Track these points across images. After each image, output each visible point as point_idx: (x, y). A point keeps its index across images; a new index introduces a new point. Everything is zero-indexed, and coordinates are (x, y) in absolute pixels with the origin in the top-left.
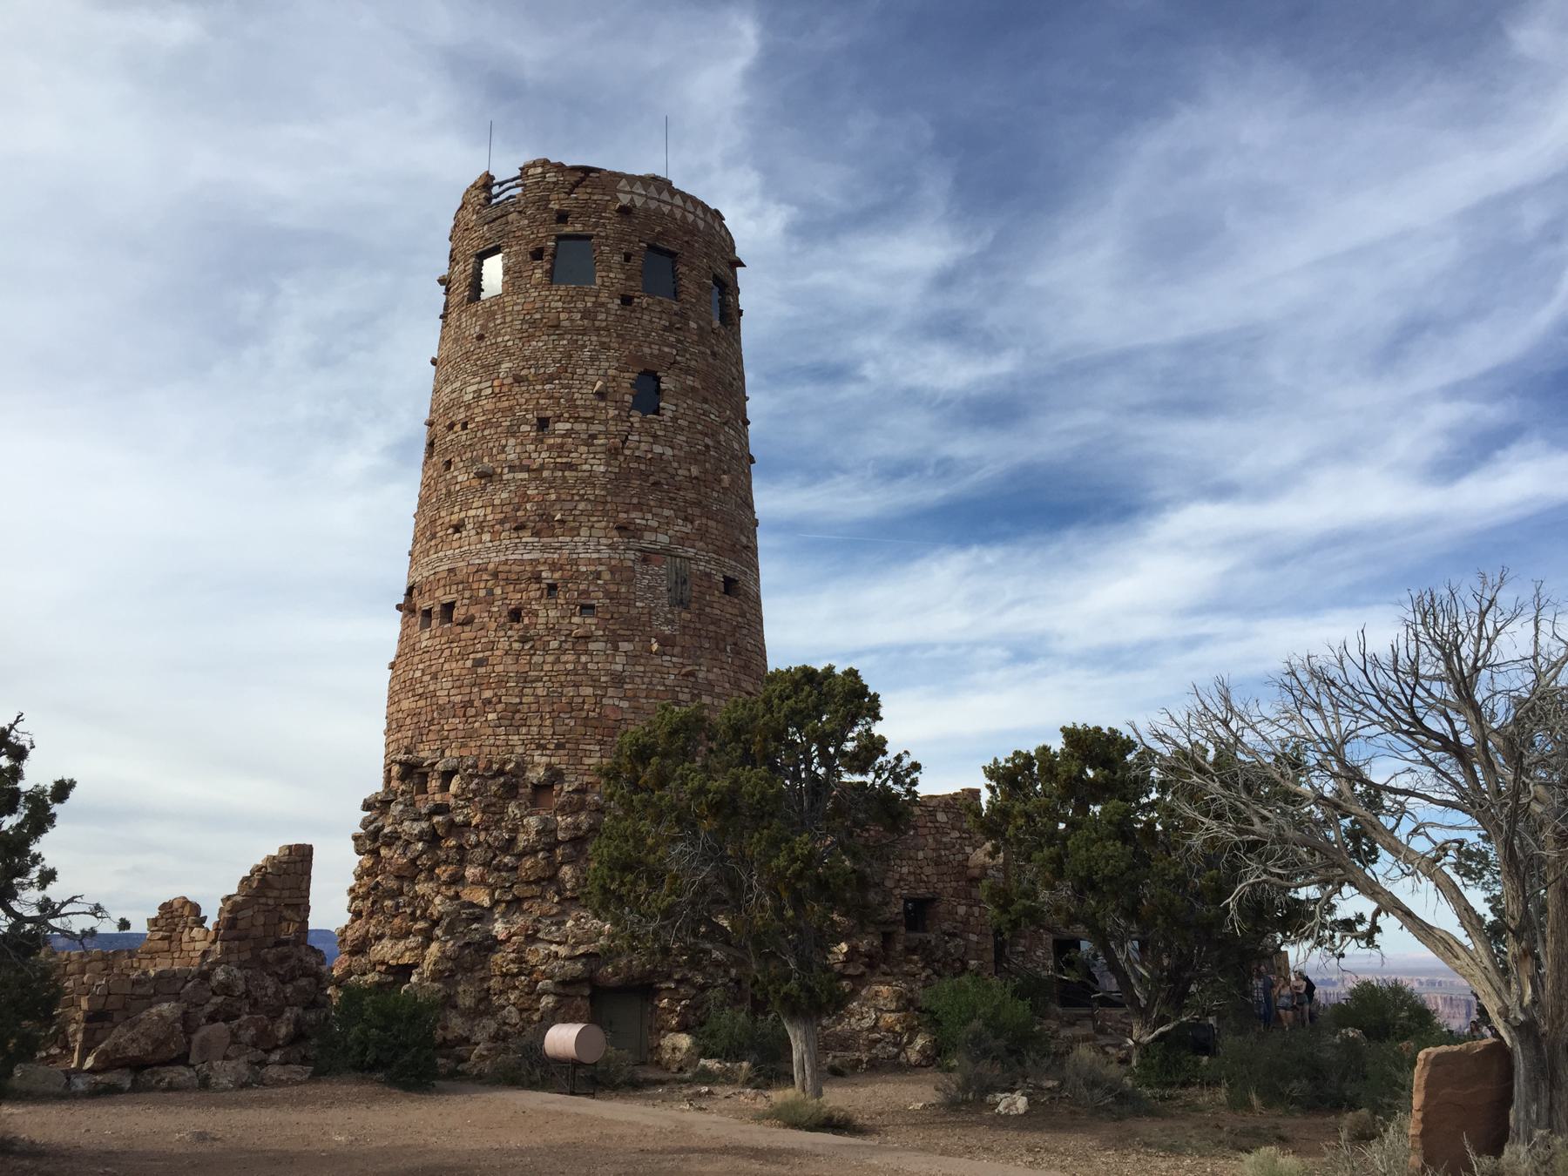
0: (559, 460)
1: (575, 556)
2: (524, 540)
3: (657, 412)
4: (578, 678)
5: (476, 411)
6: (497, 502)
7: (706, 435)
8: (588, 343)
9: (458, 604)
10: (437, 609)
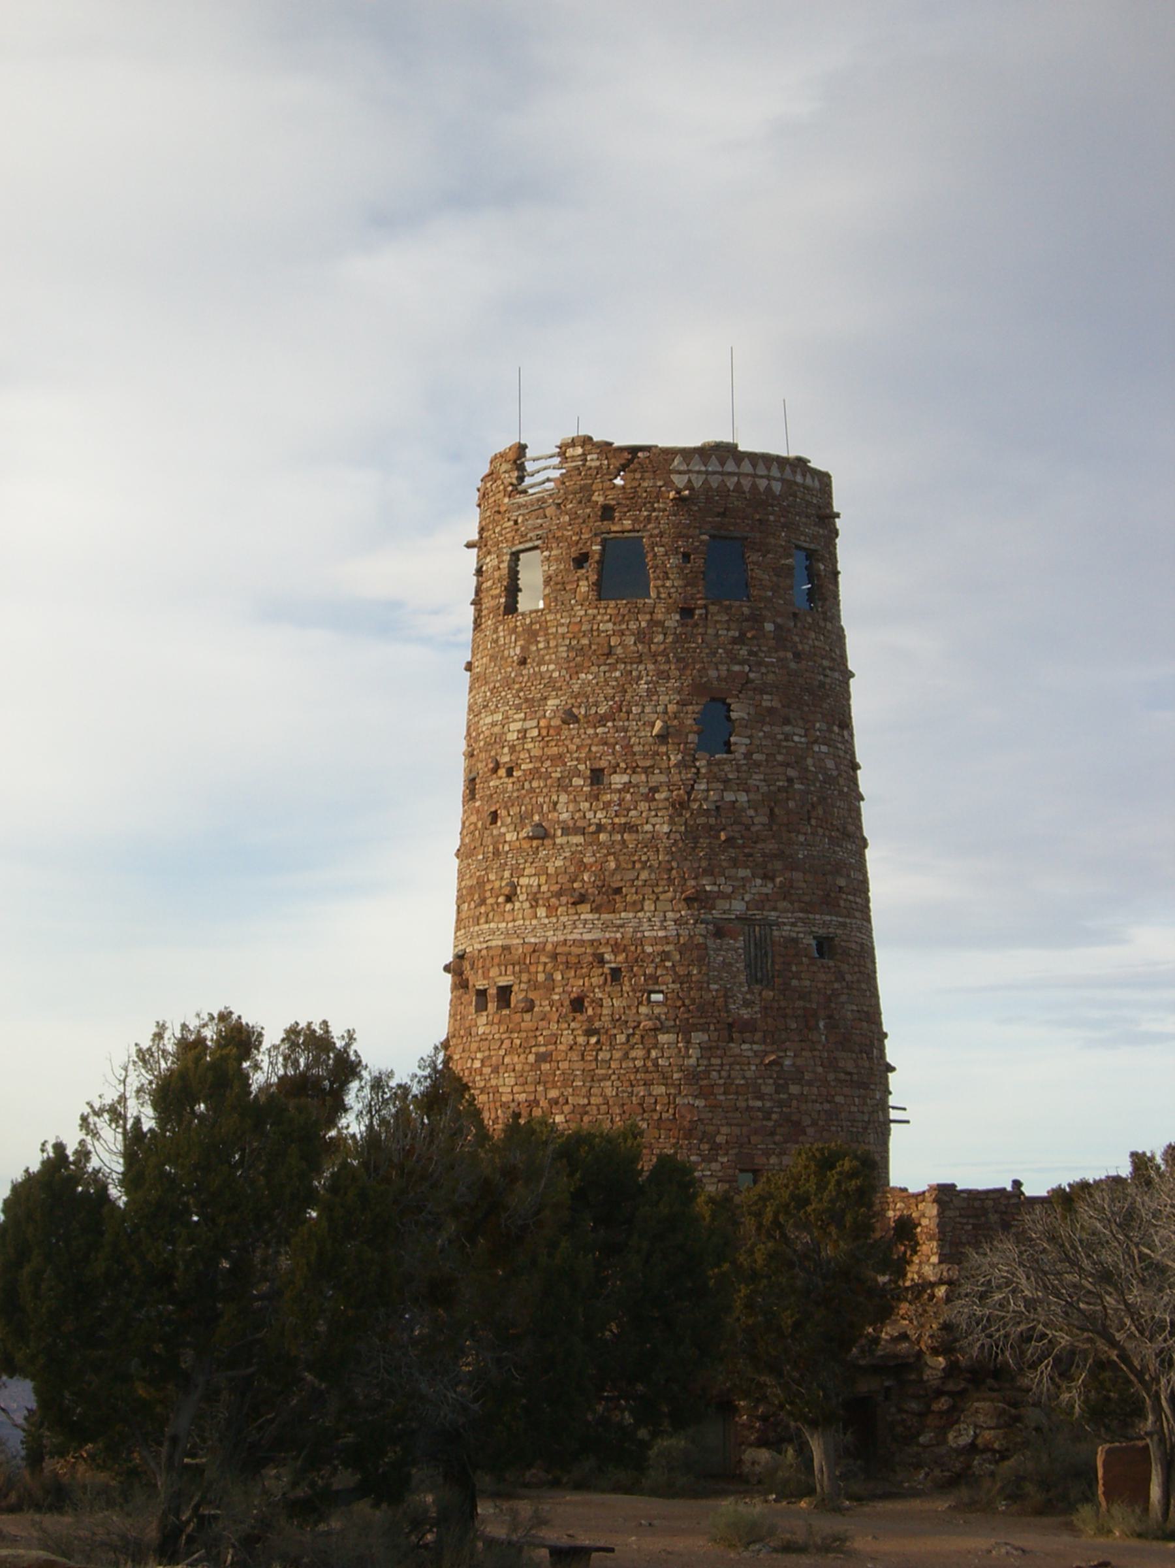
0: (616, 820)
1: (639, 935)
2: (582, 917)
3: (728, 747)
4: (648, 1076)
5: (522, 756)
6: (551, 870)
7: (788, 765)
8: (644, 673)
9: (515, 988)
10: (493, 991)
